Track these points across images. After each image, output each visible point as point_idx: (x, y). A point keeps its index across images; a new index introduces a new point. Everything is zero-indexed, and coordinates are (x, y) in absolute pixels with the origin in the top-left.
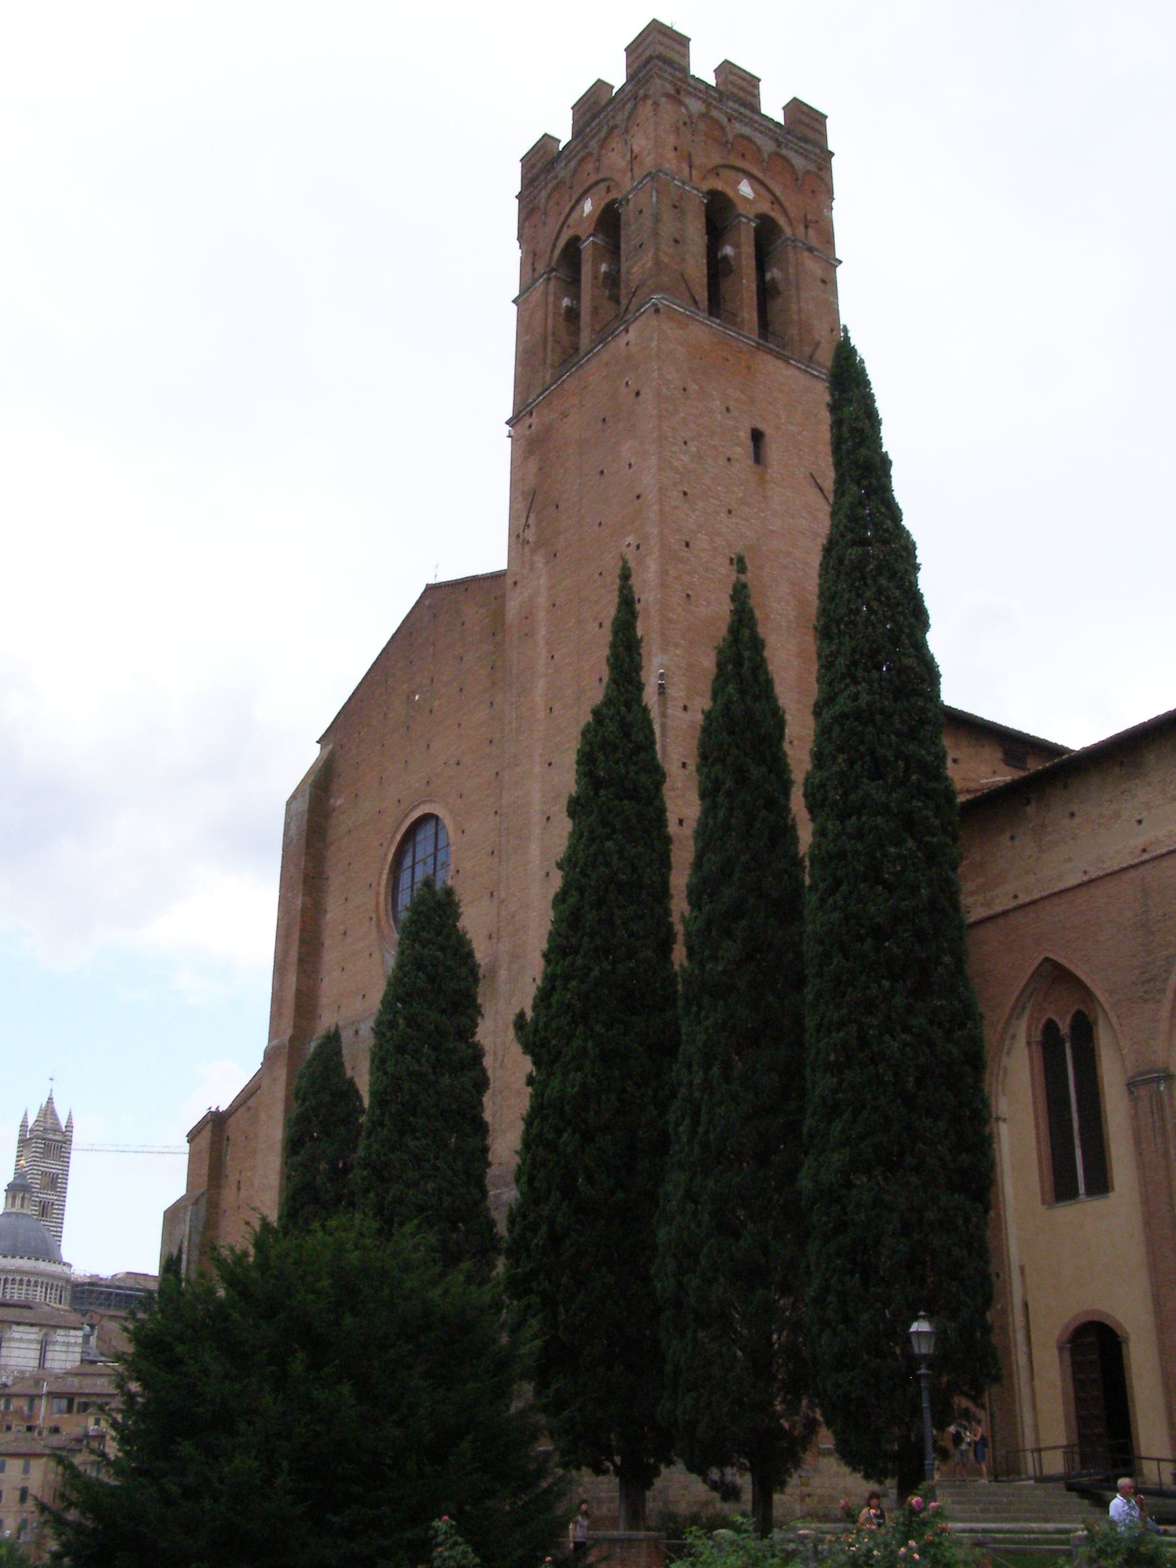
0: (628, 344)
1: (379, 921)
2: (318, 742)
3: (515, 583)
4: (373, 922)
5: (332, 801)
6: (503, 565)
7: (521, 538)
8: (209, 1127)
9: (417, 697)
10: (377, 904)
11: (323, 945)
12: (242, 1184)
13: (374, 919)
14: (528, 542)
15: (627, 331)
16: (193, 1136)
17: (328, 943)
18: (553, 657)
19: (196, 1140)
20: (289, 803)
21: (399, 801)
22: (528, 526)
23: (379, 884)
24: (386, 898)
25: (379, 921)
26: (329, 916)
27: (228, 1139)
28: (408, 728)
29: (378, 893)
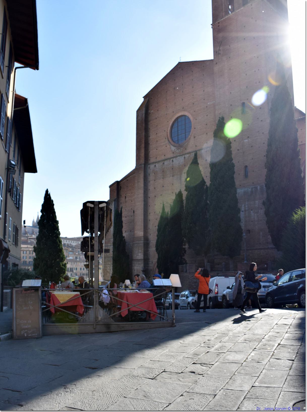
0: (252, 8)
1: (168, 138)
2: (143, 97)
3: (216, 63)
4: (167, 139)
5: (149, 111)
6: (213, 58)
7: (218, 53)
8: (116, 184)
9: (177, 88)
10: (167, 135)
11: (149, 144)
12: (126, 197)
13: (167, 138)
14: (220, 54)
15: (252, 5)
16: (110, 187)
17: (150, 144)
18: (230, 81)
19: (112, 187)
20: (138, 111)
21: (173, 112)
22: (220, 50)
23: (167, 130)
24: (170, 134)
25: (168, 138)
26: (151, 137)
27: (121, 187)
28: (175, 95)
29: (167, 133)
